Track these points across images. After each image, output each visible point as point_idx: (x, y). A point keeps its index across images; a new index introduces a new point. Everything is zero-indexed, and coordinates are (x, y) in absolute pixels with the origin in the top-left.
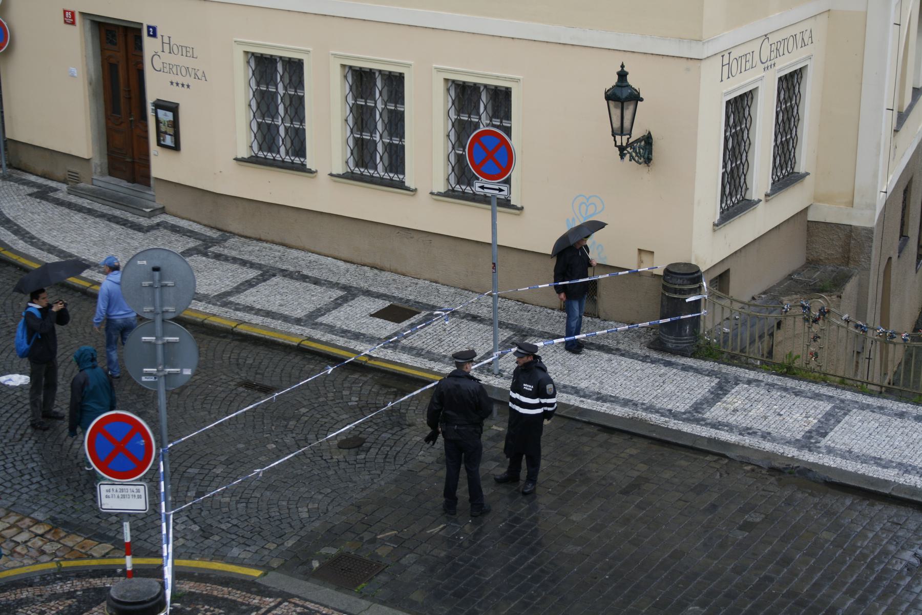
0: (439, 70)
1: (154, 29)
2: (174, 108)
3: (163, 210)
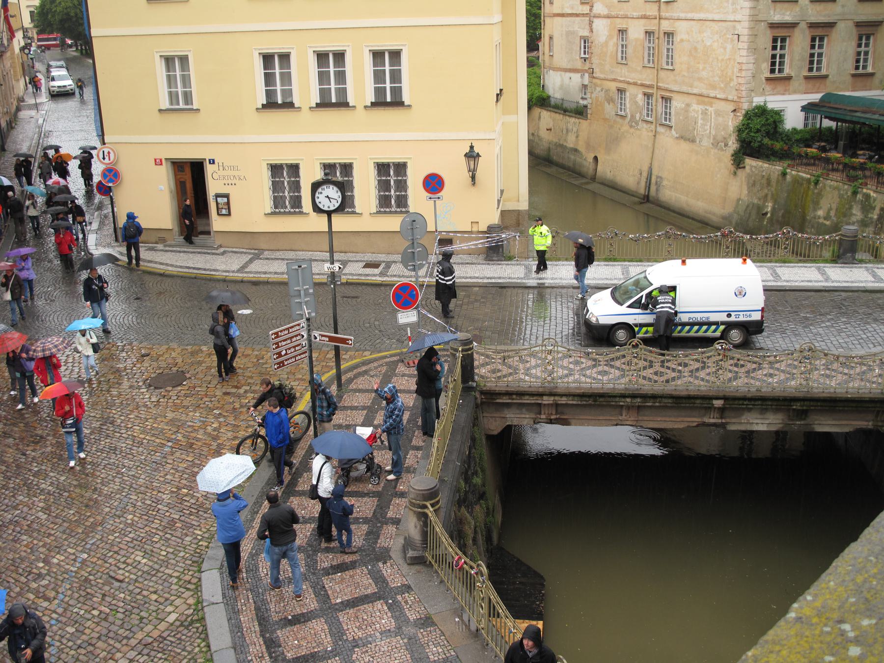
0: (371, 159)
1: (214, 161)
2: (227, 196)
3: (221, 246)
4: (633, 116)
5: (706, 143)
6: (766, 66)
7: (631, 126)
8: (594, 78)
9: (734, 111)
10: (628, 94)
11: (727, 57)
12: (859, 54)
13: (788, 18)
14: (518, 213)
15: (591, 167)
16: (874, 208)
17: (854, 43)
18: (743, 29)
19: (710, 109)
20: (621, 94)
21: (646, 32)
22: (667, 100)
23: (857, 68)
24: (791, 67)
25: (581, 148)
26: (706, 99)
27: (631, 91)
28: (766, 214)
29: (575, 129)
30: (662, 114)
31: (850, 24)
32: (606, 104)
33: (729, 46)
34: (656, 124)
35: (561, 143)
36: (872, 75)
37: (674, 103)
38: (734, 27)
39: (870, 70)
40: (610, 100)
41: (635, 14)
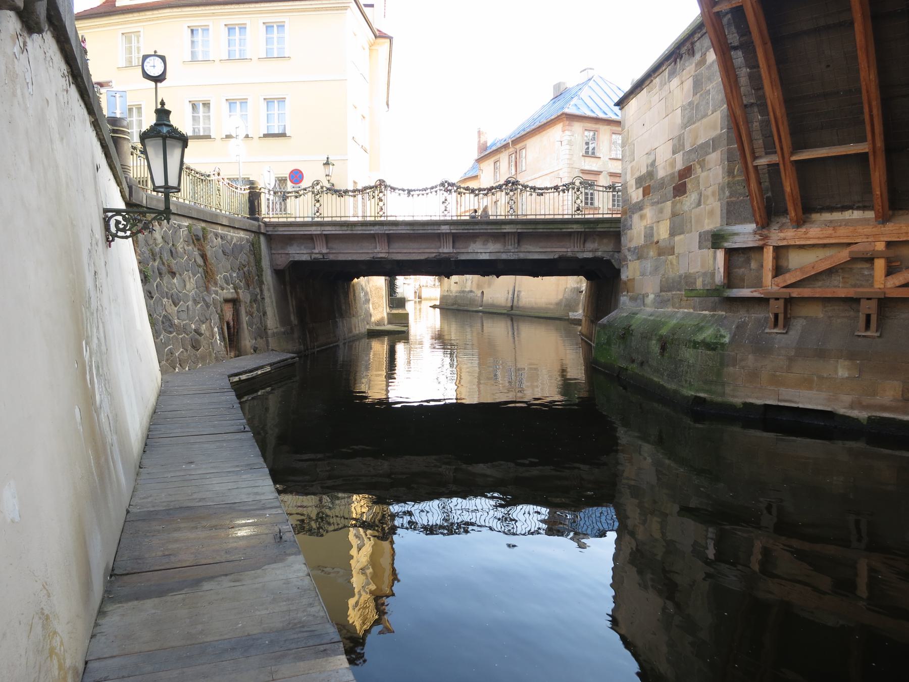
28: (582, 292)
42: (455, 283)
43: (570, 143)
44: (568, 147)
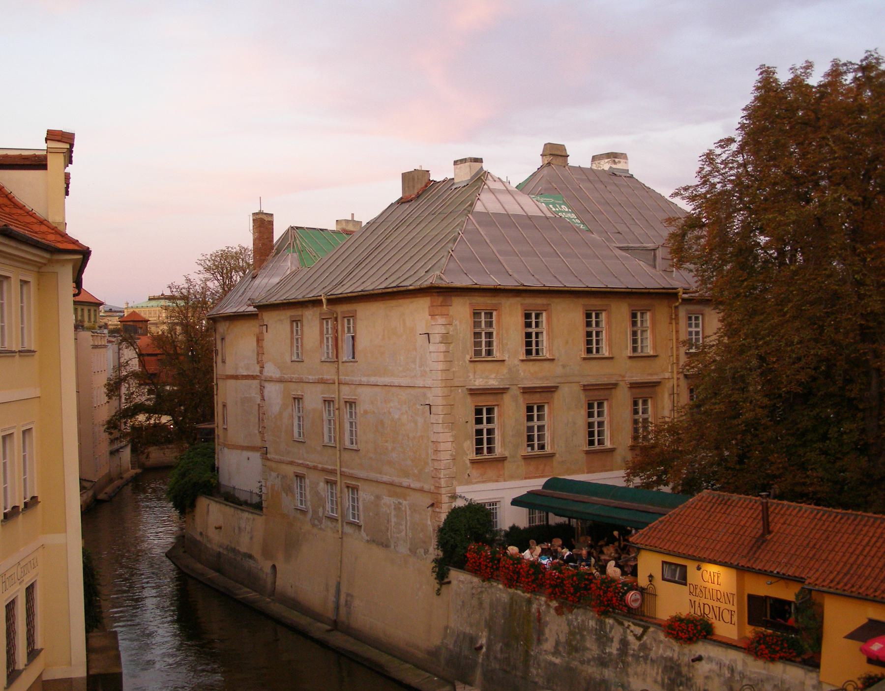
4: (315, 512)
5: (403, 549)
6: (469, 445)
7: (314, 525)
8: (268, 459)
9: (432, 505)
10: (307, 481)
11: (419, 434)
12: (590, 425)
13: (493, 383)
14: (69, 682)
15: (269, 580)
16: (612, 640)
17: (583, 412)
18: (436, 397)
19: (404, 502)
20: (301, 482)
21: (325, 401)
22: (354, 489)
23: (591, 443)
24: (503, 444)
25: (256, 552)
26: (398, 490)
27: (311, 478)
28: (481, 647)
29: (248, 529)
30: (348, 508)
31: (576, 388)
32: (284, 495)
33: (420, 420)
34: (342, 522)
35: (233, 546)
36: (612, 450)
37: (361, 493)
38: (424, 395)
39: (608, 444)
40: (289, 490)
41: (311, 378)
42: (216, 528)
43: (446, 339)
44: (442, 347)
